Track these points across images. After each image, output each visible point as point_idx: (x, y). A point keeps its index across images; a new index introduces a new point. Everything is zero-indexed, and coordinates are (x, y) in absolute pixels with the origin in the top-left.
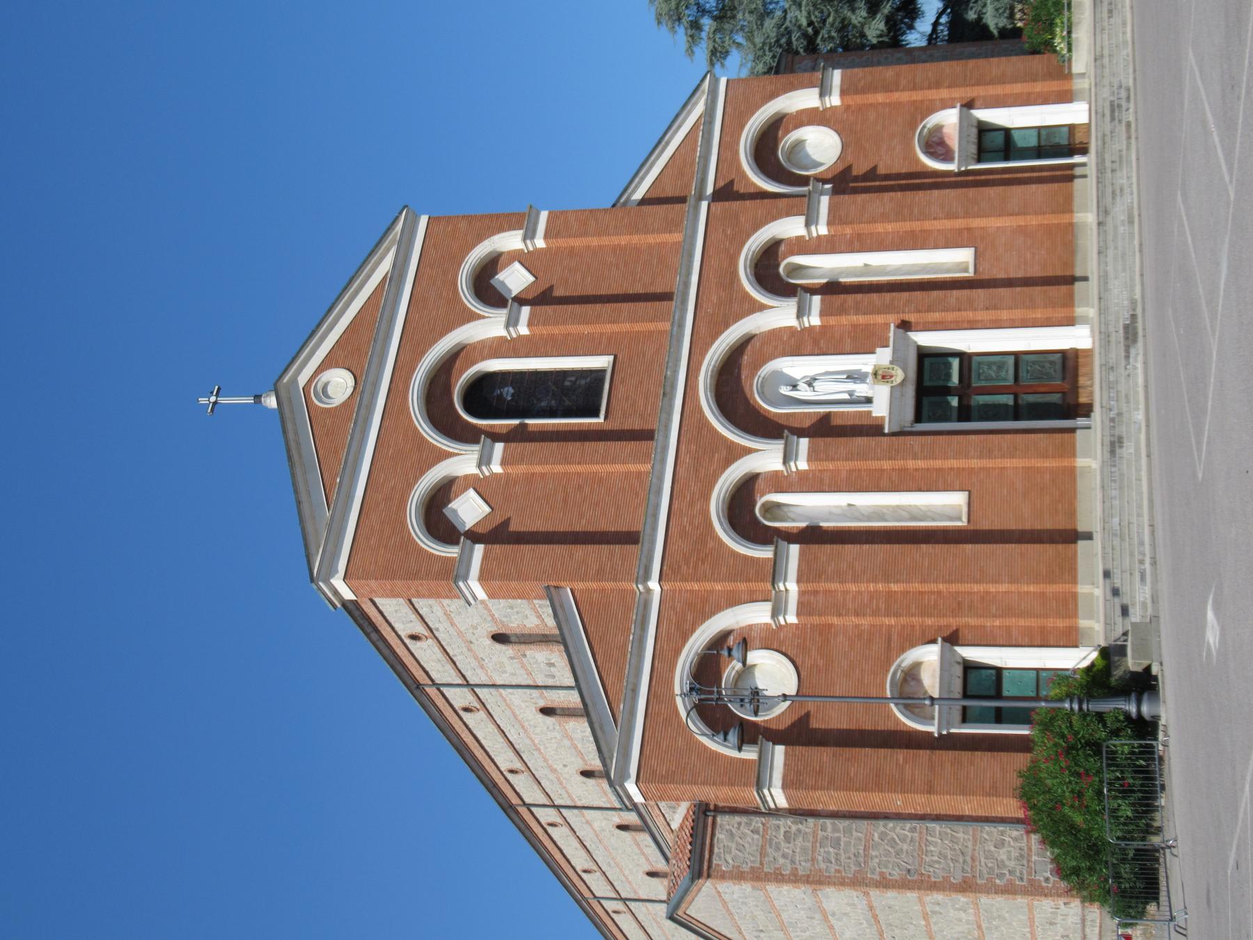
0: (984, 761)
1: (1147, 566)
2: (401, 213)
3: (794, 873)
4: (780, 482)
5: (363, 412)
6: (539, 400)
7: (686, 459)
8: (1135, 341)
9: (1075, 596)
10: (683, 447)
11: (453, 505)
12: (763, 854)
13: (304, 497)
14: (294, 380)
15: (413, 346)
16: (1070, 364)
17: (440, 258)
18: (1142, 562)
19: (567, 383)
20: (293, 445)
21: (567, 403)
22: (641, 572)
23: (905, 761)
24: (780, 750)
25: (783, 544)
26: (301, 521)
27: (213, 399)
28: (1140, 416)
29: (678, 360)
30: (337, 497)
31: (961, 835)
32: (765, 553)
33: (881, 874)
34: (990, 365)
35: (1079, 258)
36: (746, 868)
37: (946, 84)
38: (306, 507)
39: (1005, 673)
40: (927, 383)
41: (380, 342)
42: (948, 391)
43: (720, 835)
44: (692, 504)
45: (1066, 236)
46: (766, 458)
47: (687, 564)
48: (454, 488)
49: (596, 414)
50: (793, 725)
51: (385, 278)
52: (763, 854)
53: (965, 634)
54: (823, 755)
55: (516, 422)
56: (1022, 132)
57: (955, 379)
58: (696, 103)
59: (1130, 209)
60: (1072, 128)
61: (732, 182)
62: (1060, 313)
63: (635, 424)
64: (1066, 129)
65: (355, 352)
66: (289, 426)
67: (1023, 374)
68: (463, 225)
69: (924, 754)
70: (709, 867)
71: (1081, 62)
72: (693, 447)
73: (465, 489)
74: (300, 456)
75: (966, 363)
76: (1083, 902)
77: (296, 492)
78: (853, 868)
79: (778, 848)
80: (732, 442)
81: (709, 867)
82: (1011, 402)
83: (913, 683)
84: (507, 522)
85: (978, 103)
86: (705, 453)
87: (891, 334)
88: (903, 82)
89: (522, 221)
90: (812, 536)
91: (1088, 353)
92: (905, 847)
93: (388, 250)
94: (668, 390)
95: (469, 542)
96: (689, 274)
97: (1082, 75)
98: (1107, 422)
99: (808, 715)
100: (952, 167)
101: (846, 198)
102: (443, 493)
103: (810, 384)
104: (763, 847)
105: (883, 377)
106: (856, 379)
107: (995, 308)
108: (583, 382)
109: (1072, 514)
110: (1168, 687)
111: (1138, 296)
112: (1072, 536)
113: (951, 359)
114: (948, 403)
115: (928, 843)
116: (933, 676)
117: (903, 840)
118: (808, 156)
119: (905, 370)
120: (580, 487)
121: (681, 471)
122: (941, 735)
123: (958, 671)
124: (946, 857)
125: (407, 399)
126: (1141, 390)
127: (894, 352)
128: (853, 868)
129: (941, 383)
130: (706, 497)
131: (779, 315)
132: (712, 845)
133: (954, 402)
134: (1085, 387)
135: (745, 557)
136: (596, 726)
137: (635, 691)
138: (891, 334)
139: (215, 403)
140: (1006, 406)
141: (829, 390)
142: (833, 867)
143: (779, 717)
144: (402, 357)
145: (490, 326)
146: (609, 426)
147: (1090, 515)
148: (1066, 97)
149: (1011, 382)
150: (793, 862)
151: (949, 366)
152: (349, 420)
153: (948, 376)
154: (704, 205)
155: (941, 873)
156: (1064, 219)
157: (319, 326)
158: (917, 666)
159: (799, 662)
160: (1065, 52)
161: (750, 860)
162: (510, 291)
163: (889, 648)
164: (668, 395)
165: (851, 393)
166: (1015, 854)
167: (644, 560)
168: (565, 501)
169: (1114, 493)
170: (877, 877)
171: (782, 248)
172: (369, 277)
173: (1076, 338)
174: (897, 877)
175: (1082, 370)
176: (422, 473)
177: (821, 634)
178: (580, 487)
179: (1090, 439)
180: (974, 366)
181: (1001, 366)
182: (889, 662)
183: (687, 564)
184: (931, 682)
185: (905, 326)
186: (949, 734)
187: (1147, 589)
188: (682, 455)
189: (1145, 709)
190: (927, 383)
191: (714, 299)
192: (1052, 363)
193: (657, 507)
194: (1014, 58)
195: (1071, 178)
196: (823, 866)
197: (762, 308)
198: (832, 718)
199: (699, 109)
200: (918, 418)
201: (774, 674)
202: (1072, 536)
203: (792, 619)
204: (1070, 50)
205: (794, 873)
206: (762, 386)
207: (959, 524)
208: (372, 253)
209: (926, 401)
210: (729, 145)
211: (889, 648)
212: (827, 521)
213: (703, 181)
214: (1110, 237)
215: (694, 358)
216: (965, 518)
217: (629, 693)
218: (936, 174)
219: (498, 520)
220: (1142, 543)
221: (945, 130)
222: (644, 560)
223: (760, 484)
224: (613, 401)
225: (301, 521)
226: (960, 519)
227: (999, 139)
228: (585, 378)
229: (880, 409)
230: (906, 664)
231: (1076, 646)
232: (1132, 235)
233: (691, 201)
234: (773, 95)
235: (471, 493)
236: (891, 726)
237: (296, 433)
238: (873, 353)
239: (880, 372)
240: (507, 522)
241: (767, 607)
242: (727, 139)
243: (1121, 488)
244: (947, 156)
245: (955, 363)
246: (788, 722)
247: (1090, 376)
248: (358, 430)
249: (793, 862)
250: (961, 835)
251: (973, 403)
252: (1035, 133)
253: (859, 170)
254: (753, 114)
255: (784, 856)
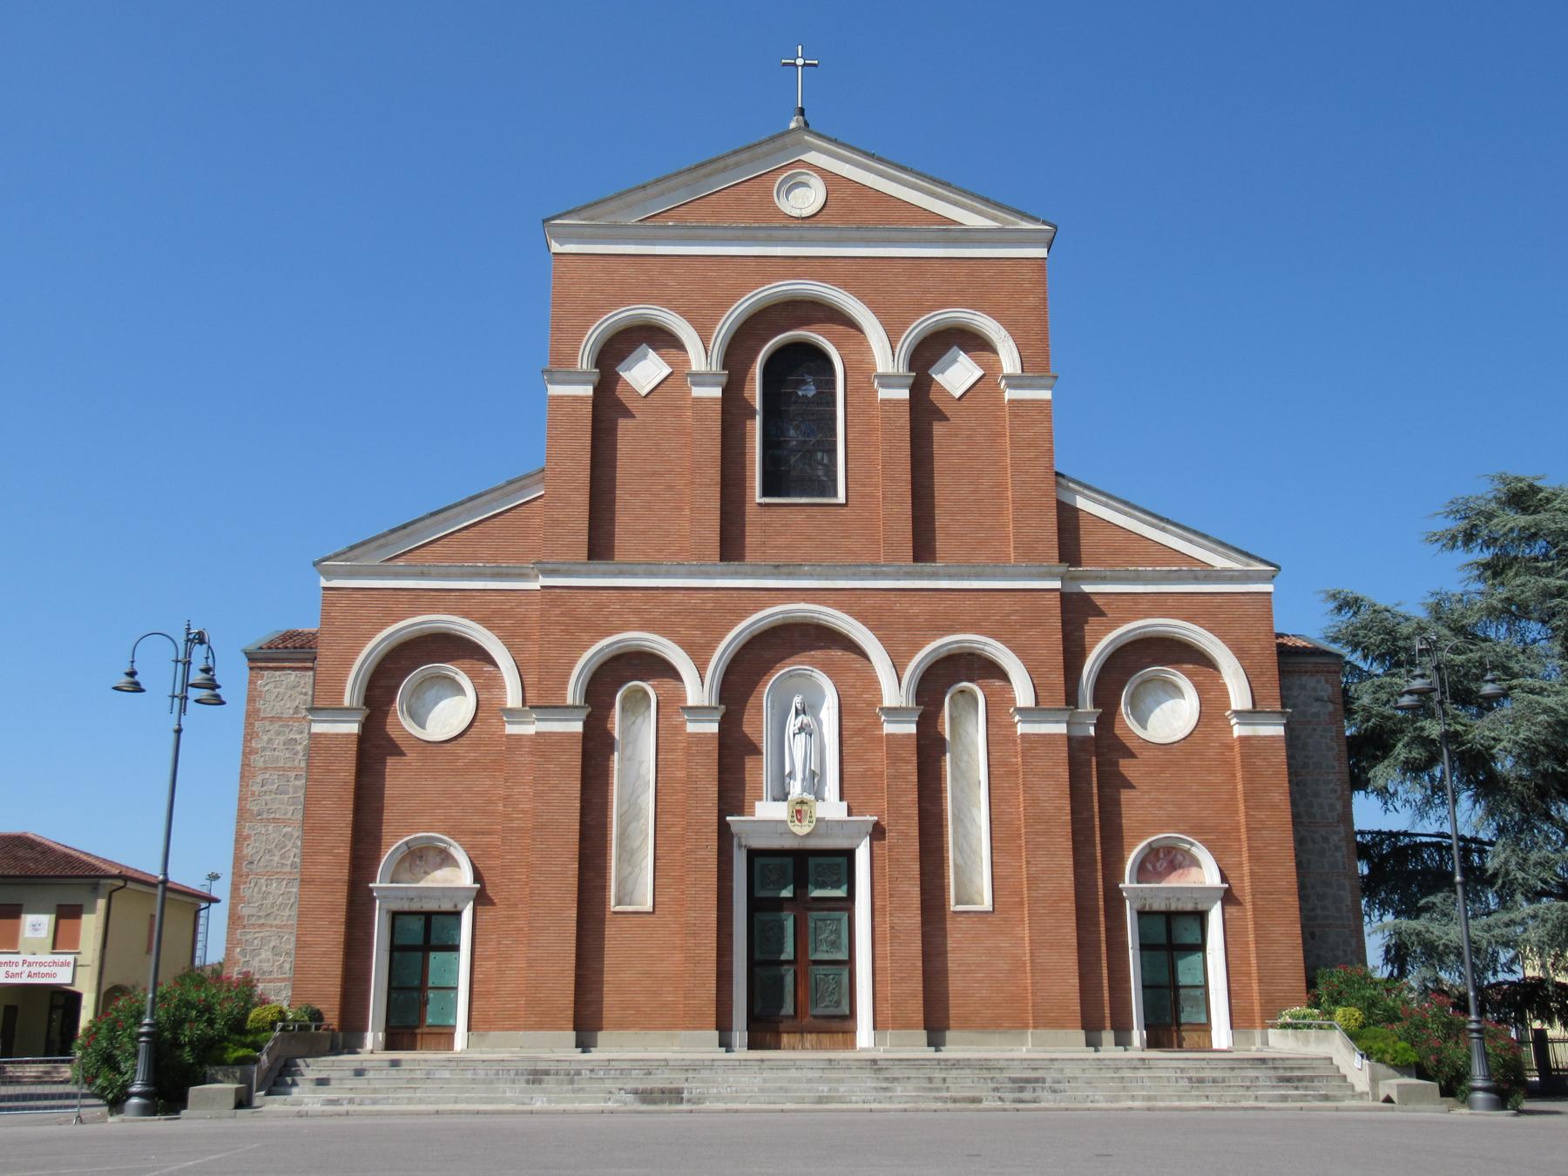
0: (331, 936)
1: (345, 1107)
2: (1044, 223)
3: (253, 752)
4: (672, 706)
5: (761, 234)
6: (797, 428)
7: (696, 599)
8: (644, 1101)
9: (1026, 1027)
10: (711, 595)
11: (652, 353)
12: (272, 719)
13: (651, 191)
14: (809, 148)
15: (852, 274)
16: (835, 1025)
17: (978, 282)
18: (351, 1101)
19: (819, 455)
20: (721, 164)
21: (793, 459)
22: (549, 567)
23: (338, 855)
24: (577, 727)
25: (583, 714)
26: (620, 195)
27: (800, 62)
28: (538, 1105)
29: (827, 577)
30: (652, 229)
31: (287, 913)
32: (573, 693)
33: (248, 837)
34: (837, 932)
35: (973, 1035)
36: (259, 704)
37: (1256, 869)
38: (641, 195)
39: (1197, 957)
40: (812, 861)
41: (857, 234)
42: (801, 884)
43: (292, 677)
44: (637, 611)
45: (1009, 1017)
46: (698, 689)
47: (562, 614)
48: (673, 351)
49: (765, 493)
50: (391, 740)
51: (955, 222)
52: (272, 719)
53: (487, 914)
54: (345, 772)
55: (758, 405)
56: (1201, 966)
57: (817, 893)
58: (1229, 558)
59: (979, 1100)
60: (1206, 1027)
61: (1101, 613)
62: (886, 1009)
63: (752, 537)
64: (1203, 1020)
65: (849, 209)
66: (744, 156)
67: (822, 970)
68: (1032, 300)
69: (344, 874)
70: (261, 668)
71: (1281, 1043)
72: (710, 606)
73: (670, 364)
74: (710, 175)
75: (842, 904)
76: (601, 1029)
77: (657, 181)
78: (255, 809)
79: (278, 734)
80: (714, 649)
81: (261, 668)
82: (784, 957)
83: (438, 859)
84: (628, 414)
85: (1232, 910)
86: (697, 620)
87: (868, 818)
88: (1261, 815)
89: (1036, 366)
90: (596, 748)
91: (850, 1044)
92: (276, 859)
93: (994, 219)
94: (784, 570)
95: (910, 381)
96: (951, 577)
97: (1265, 1042)
98: (574, 1067)
99: (402, 754)
100: (1127, 883)
101: (1063, 754)
102: (661, 338)
103: (801, 729)
104: (280, 718)
105: (799, 812)
106: (807, 783)
107: (893, 937)
108: (820, 473)
109: (621, 1025)
110: (159, 1125)
111: (707, 1105)
112: (586, 1027)
113: (845, 887)
114: (784, 887)
115: (280, 881)
116: (446, 880)
117: (282, 857)
118: (1159, 703)
119: (808, 835)
120: (671, 488)
121: (679, 596)
122: (371, 890)
123: (447, 906)
124: (264, 898)
125: (783, 278)
126: (561, 1107)
127: (840, 823)
128: (255, 809)
129: (811, 878)
130: (647, 626)
131: (894, 690)
132: (283, 668)
133: (787, 893)
134: (802, 1041)
135: (568, 675)
136: (382, 541)
137: (423, 575)
138: (868, 818)
139: (795, 65)
140: (781, 951)
141: (797, 748)
142: (256, 788)
143: (399, 724)
144: (840, 263)
145: (885, 356)
146: (751, 513)
147: (956, 1048)
148: (1238, 1020)
149: (813, 958)
150: (264, 749)
151: (836, 886)
152: (756, 221)
153: (823, 886)
154: (1057, 584)
155: (248, 894)
156: (1258, 1021)
157: (880, 160)
158: (1195, 863)
159: (461, 741)
160: (1281, 1021)
161: (267, 708)
162: (629, 369)
163: (475, 833)
164: (777, 570)
165: (791, 775)
166: (266, 966)
167: (565, 567)
168: (654, 473)
169: (482, 1073)
170: (246, 832)
171: (998, 683)
172: (955, 203)
173: (1221, 1035)
174: (245, 851)
175: (825, 1038)
176: (683, 314)
177: (493, 761)
178: (671, 488)
179: (559, 1046)
180: (837, 914)
181: (834, 945)
182: (455, 832)
183: (562, 614)
184: (440, 878)
185: (877, 832)
186: (374, 899)
187: (318, 1107)
188: (700, 595)
189: (135, 1101)
190: (812, 861)
191: (916, 610)
192: (838, 1004)
193: (634, 575)
194: (1300, 954)
195: (1092, 1030)
196: (259, 779)
197: (898, 669)
198: (397, 779)
199: (1219, 562)
200: (753, 854)
201: (448, 716)
202: (586, 1027)
203: (1238, 731)
204: (1285, 1026)
205: (253, 752)
206: (800, 675)
207: (613, 902)
208: (986, 201)
209: (789, 861)
210: (1159, 605)
211: (475, 833)
212: (621, 760)
213: (1103, 579)
214: (811, 1074)
215: (832, 595)
216: (618, 908)
217: (418, 570)
218: (1121, 860)
219: (629, 406)
220: (374, 1102)
221: (1194, 870)
222: (565, 567)
223: (669, 684)
224: (785, 510)
225: (620, 195)
226: (619, 903)
227: (1191, 938)
228: (826, 474)
229: (767, 810)
230: (452, 851)
231: (469, 1029)
232: (801, 1100)
233: (1063, 568)
234: (1240, 653)
235: (979, 373)
236: (385, 839)
237: (738, 165)
238: (841, 799)
239: (805, 807)
240: (628, 414)
241: (1030, 703)
242: (1170, 601)
243: (484, 1082)
244: (1142, 872)
245: (841, 893)
246: (391, 730)
247: (818, 1047)
248: (739, 233)
249: (264, 749)
250: (287, 913)
251: (784, 914)
252: (1199, 981)
253: (1127, 767)
254: (1210, 630)
255: (270, 740)
